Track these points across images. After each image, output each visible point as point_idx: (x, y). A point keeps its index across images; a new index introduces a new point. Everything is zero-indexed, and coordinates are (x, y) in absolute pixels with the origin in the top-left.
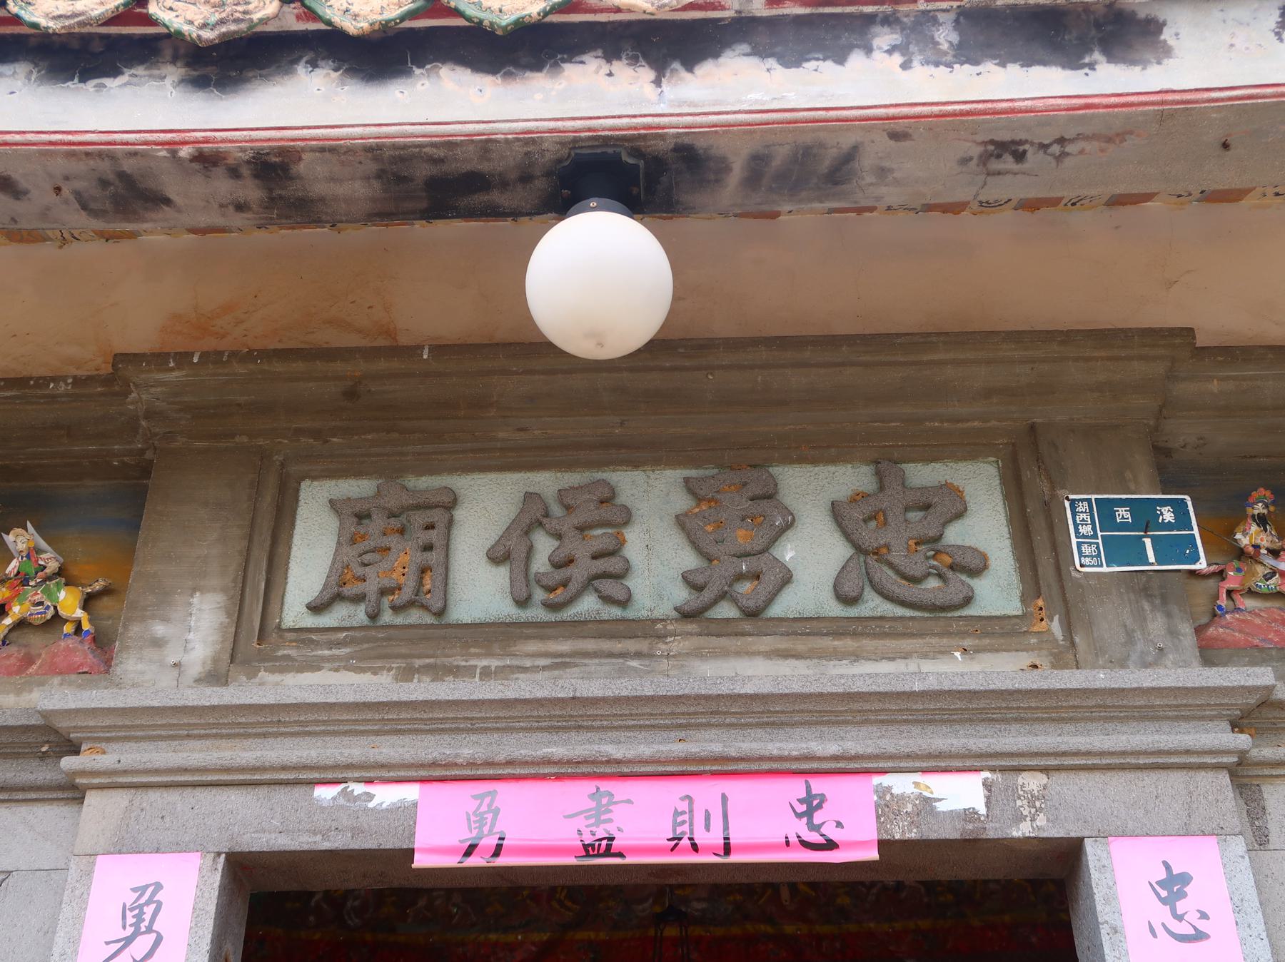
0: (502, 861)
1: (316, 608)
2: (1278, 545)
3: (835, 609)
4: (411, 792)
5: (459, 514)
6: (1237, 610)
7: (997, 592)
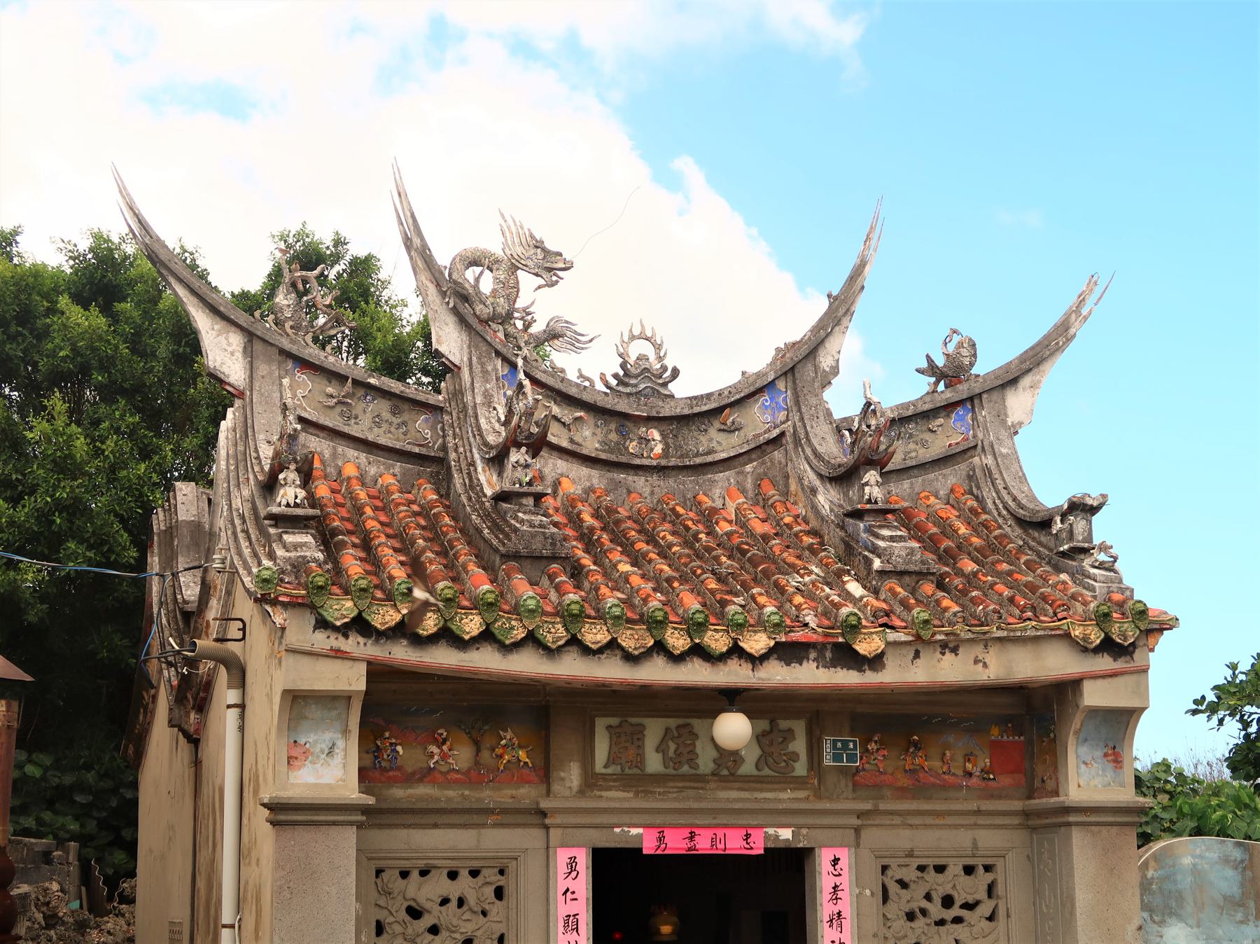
0: (666, 852)
1: (605, 767)
3: (755, 772)
4: (641, 831)
5: (646, 733)
7: (800, 768)
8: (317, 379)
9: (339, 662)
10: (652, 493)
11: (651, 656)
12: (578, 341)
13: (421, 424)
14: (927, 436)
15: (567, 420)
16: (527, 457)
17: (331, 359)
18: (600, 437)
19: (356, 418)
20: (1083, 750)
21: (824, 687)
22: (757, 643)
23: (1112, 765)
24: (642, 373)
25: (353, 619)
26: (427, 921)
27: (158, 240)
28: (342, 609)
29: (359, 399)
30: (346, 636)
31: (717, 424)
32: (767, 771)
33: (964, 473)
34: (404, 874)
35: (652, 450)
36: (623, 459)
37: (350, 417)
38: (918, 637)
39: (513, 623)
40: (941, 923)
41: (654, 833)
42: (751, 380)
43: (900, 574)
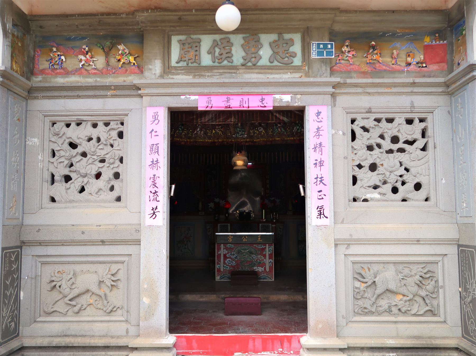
0: (212, 109)
1: (177, 63)
2: (350, 50)
3: (269, 64)
4: (197, 97)
5: (202, 43)
6: (340, 63)
7: (297, 61)
26: (80, 150)
32: (276, 63)
34: (68, 125)
40: (390, 151)
41: (205, 99)
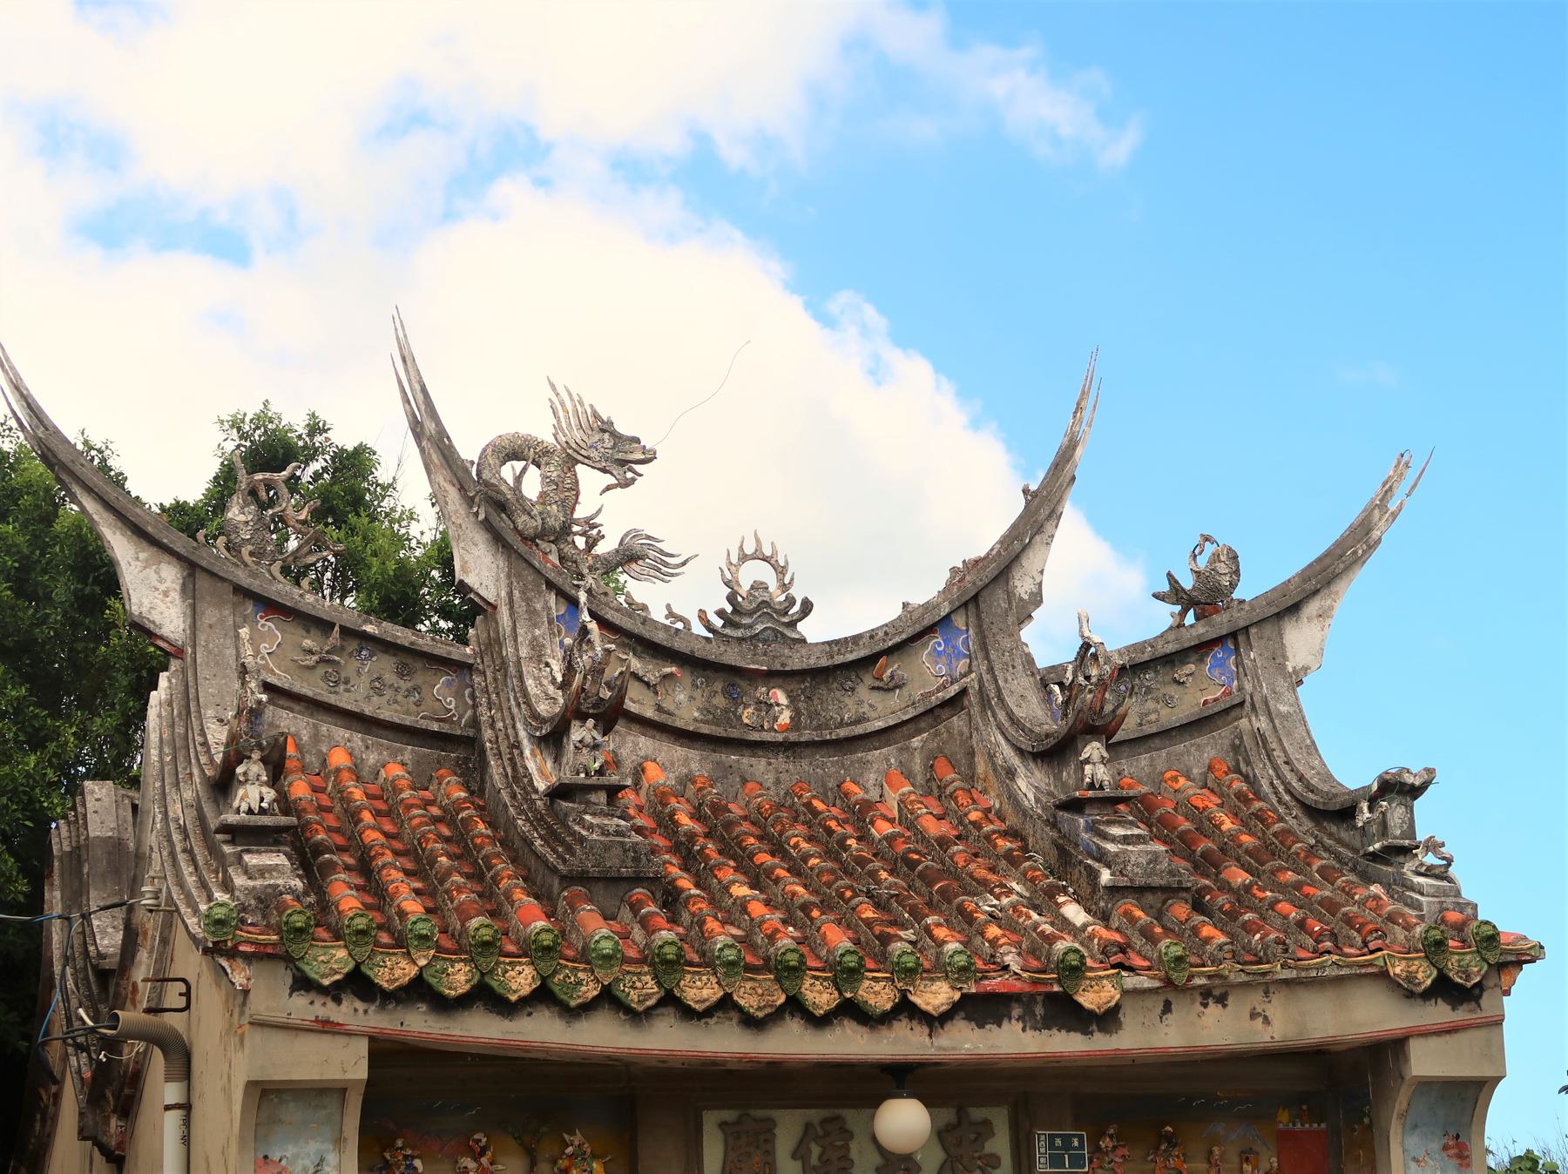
5: (777, 1131)
8: (289, 628)
9: (327, 1039)
10: (778, 782)
11: (783, 1019)
12: (666, 565)
13: (441, 691)
14: (1173, 690)
15: (652, 678)
16: (595, 733)
17: (310, 598)
18: (700, 702)
19: (347, 682)
20: (1413, 1141)
21: (1035, 1058)
22: (936, 996)
23: (1455, 1162)
24: (758, 608)
25: (348, 976)
27: (57, 432)
28: (332, 961)
29: (351, 654)
30: (338, 1001)
31: (868, 680)
33: (1227, 742)
35: (775, 719)
36: (734, 733)
37: (339, 682)
38: (1169, 983)
39: (581, 975)
42: (916, 615)
43: (1139, 891)
